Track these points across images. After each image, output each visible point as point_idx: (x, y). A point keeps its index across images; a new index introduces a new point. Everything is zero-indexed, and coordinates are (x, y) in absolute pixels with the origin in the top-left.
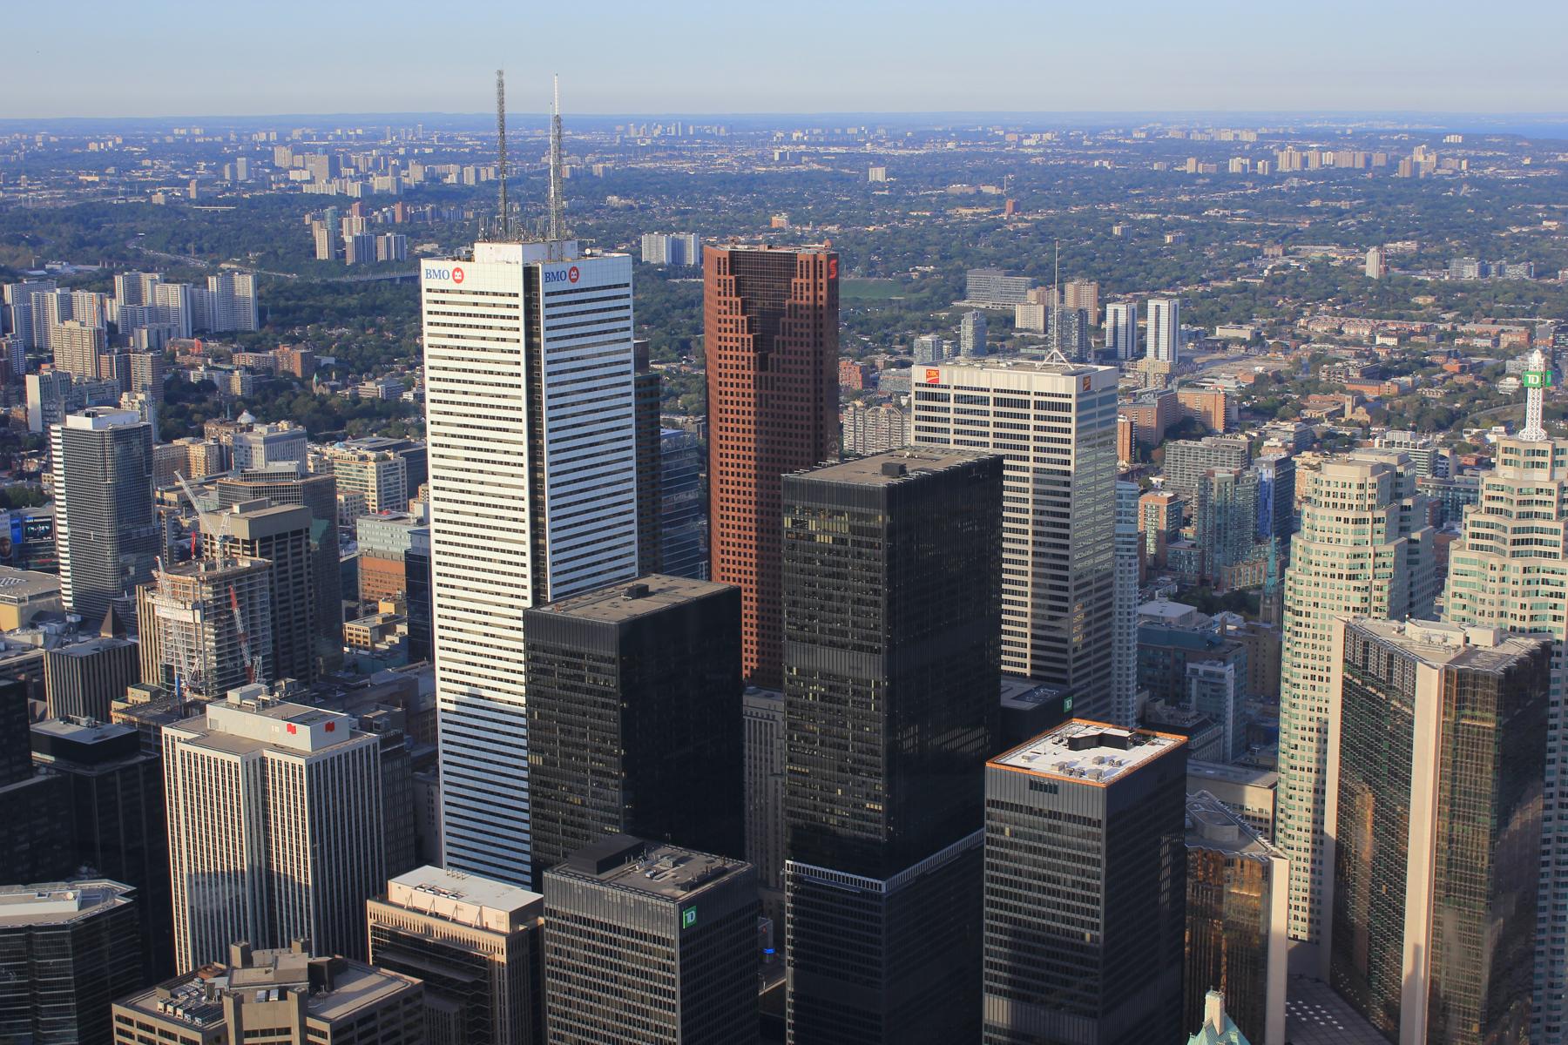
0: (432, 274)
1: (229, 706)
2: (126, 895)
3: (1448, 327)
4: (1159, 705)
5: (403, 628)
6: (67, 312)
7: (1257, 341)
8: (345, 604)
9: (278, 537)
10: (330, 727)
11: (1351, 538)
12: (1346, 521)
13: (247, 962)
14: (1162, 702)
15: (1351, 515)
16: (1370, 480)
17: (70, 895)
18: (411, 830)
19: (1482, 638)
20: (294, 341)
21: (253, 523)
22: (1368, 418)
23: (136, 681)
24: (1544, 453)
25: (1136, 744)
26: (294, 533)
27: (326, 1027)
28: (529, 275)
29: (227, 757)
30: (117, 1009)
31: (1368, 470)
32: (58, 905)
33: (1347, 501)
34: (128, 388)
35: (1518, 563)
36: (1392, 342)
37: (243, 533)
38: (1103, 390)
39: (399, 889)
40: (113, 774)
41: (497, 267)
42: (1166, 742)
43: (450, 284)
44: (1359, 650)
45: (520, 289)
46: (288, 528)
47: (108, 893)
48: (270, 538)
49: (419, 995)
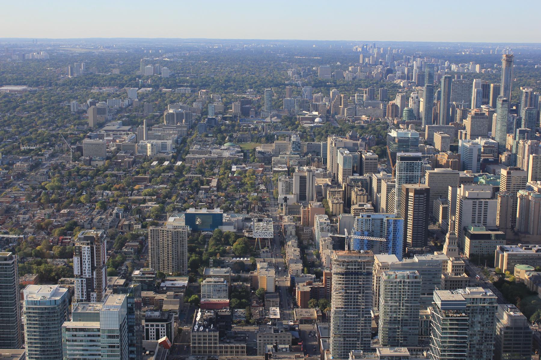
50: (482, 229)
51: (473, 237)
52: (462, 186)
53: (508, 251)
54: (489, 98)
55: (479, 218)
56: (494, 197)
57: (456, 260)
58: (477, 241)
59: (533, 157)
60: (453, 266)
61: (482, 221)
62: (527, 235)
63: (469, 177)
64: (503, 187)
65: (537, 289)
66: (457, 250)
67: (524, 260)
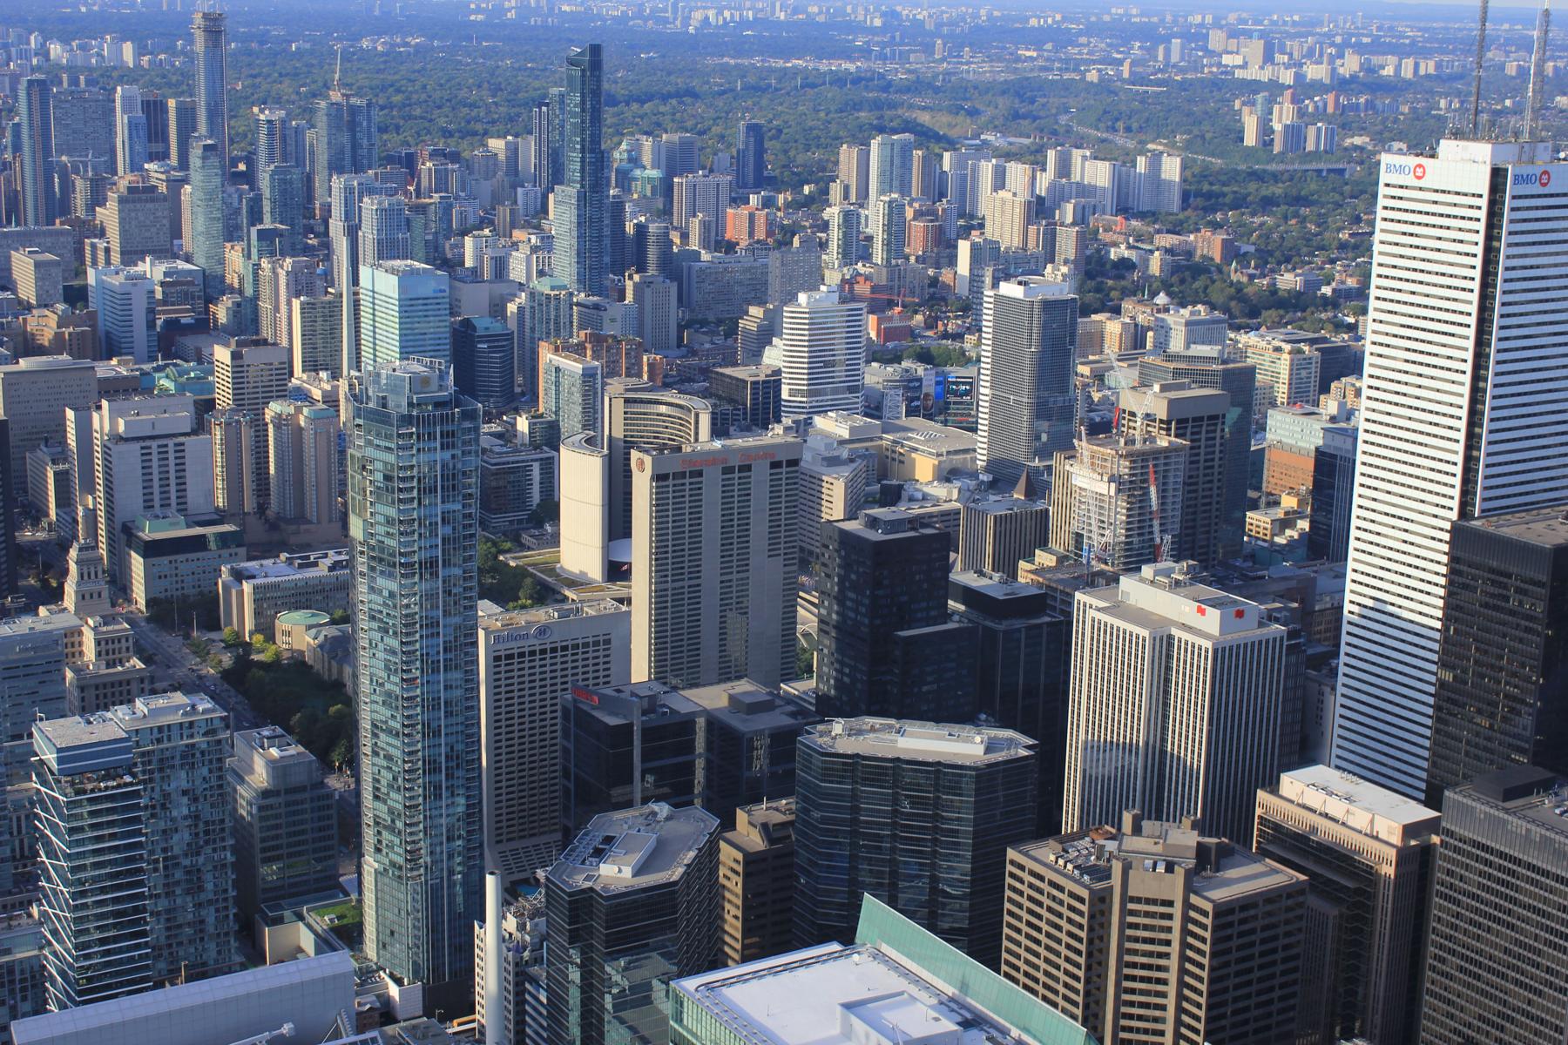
0: (1389, 168)
1: (1142, 580)
2: (1029, 747)
5: (1304, 525)
6: (1000, 182)
8: (1252, 494)
9: (1194, 420)
10: (1240, 614)
13: (1137, 830)
17: (978, 739)
18: (1298, 728)
20: (1216, 226)
21: (1171, 402)
23: (1043, 543)
26: (1210, 418)
27: (1208, 907)
28: (1497, 175)
29: (1137, 630)
30: (1011, 854)
32: (966, 746)
34: (1052, 261)
37: (1162, 414)
39: (1294, 784)
40: (1019, 630)
41: (1463, 166)
43: (1410, 180)
45: (1485, 191)
46: (1205, 414)
47: (1011, 742)
48: (1186, 421)
49: (1302, 892)
50: (174, 525)
51: (151, 550)
52: (105, 403)
53: (253, 577)
54: (166, 140)
55: (164, 492)
56: (200, 427)
57: (105, 624)
58: (165, 560)
59: (302, 304)
60: (98, 643)
61: (173, 500)
62: (303, 527)
63: (126, 378)
64: (224, 396)
65: (340, 672)
66: (105, 594)
67: (301, 598)
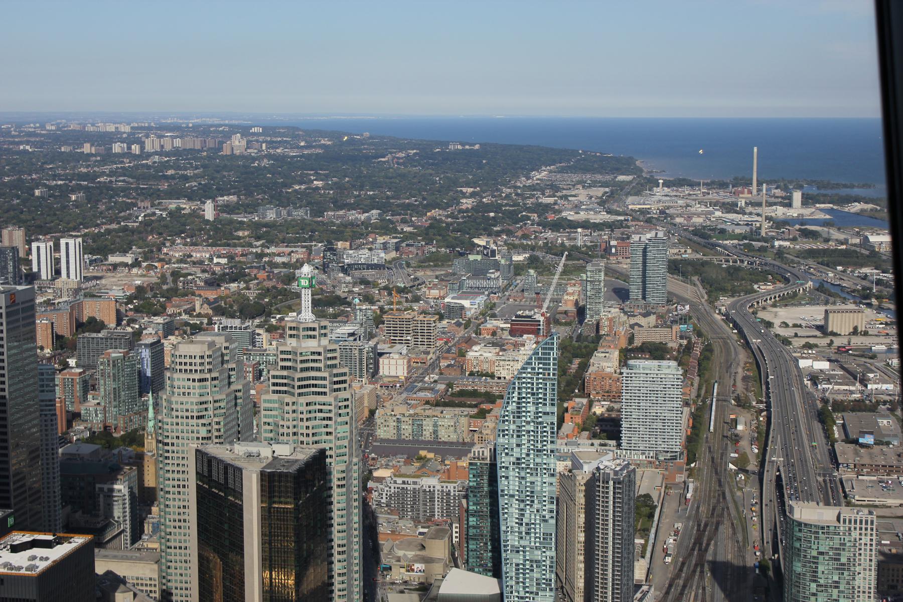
3: (259, 250)
4: (78, 515)
7: (136, 264)
11: (197, 391)
12: (194, 380)
14: (80, 513)
15: (197, 376)
16: (208, 353)
19: (283, 450)
22: (210, 312)
24: (314, 329)
25: (58, 543)
31: (206, 346)
33: (193, 368)
35: (303, 400)
36: (224, 261)
38: (23, 303)
42: (79, 540)
44: (205, 464)
